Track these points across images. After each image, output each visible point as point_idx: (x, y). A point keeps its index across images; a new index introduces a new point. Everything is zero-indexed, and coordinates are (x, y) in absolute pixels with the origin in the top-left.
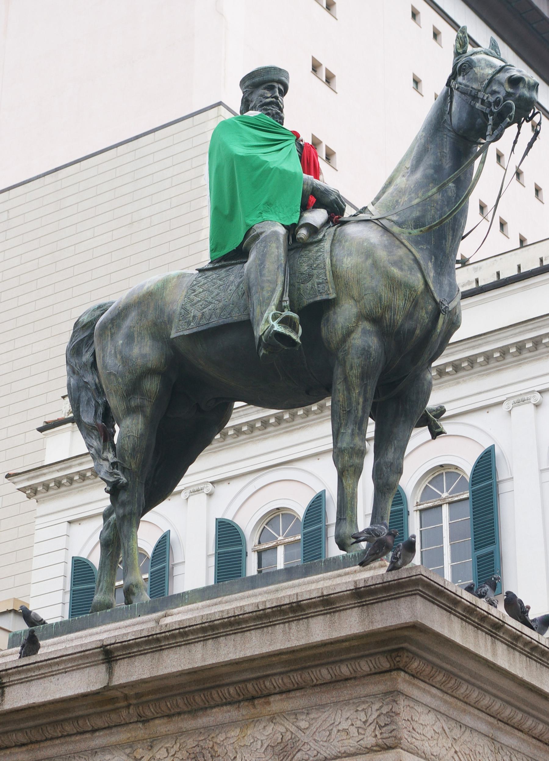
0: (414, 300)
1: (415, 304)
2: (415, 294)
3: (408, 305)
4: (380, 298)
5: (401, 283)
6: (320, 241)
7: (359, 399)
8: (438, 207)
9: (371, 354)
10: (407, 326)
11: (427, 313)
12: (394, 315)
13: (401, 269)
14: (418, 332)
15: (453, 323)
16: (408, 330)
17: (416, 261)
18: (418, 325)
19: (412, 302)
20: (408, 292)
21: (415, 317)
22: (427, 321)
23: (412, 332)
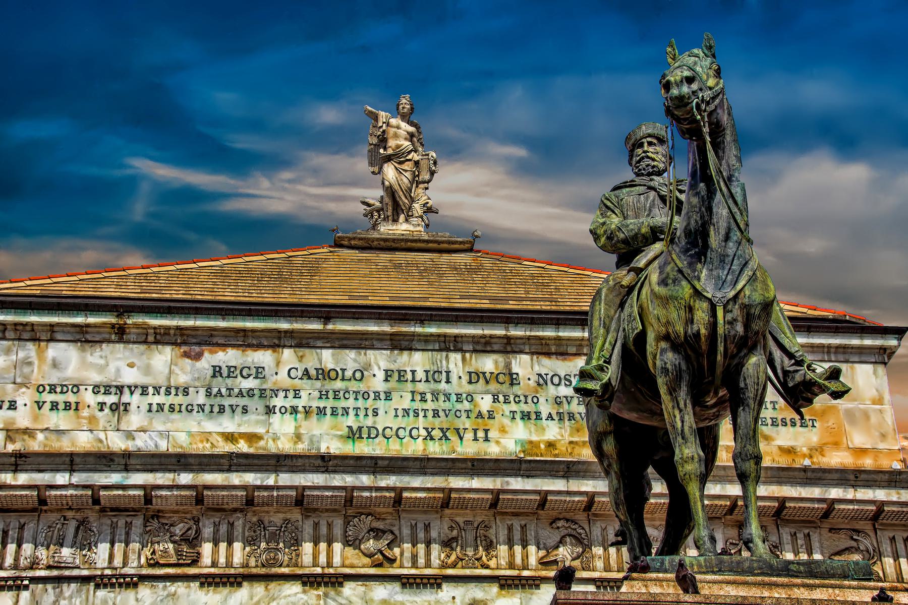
1: (690, 309)
2: (683, 302)
3: (682, 313)
11: (703, 312)
14: (703, 331)
17: (680, 271)
22: (707, 318)
23: (697, 335)
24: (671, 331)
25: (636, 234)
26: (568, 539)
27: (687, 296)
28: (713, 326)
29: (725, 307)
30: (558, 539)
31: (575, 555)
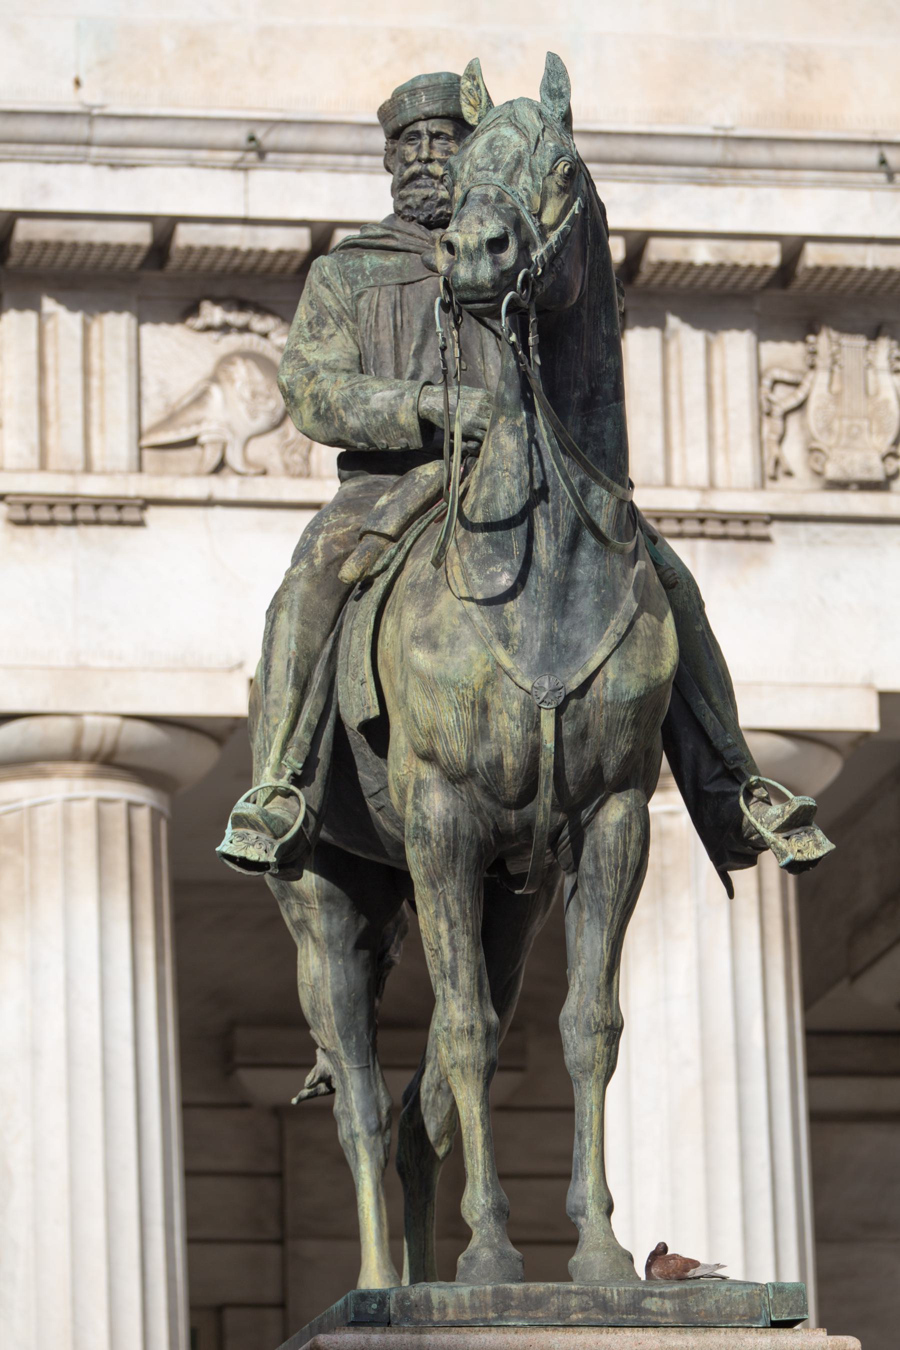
0: (473, 703)
2: (469, 693)
3: (466, 717)
4: (414, 716)
5: (434, 679)
6: (385, 568)
7: (437, 927)
8: (515, 470)
9: (429, 833)
10: (482, 757)
11: (512, 718)
12: (446, 743)
13: (434, 646)
14: (509, 760)
15: (607, 703)
16: (487, 763)
18: (503, 747)
19: (473, 708)
20: (454, 694)
21: (493, 735)
22: (518, 733)
23: (497, 765)
24: (439, 747)
25: (385, 423)
26: (241, 370)
27: (477, 681)
28: (536, 750)
29: (560, 710)
30: (207, 365)
31: (262, 421)
